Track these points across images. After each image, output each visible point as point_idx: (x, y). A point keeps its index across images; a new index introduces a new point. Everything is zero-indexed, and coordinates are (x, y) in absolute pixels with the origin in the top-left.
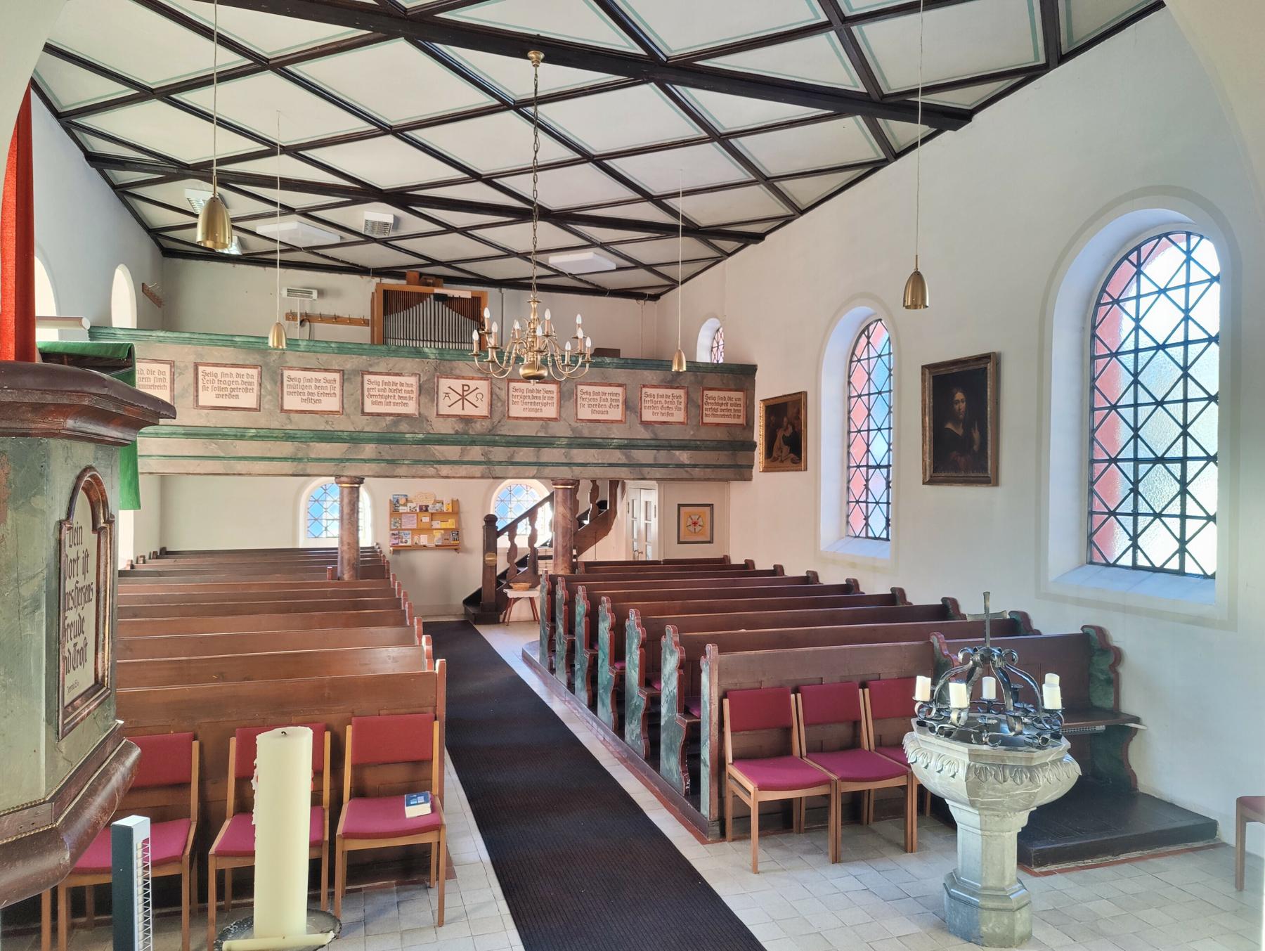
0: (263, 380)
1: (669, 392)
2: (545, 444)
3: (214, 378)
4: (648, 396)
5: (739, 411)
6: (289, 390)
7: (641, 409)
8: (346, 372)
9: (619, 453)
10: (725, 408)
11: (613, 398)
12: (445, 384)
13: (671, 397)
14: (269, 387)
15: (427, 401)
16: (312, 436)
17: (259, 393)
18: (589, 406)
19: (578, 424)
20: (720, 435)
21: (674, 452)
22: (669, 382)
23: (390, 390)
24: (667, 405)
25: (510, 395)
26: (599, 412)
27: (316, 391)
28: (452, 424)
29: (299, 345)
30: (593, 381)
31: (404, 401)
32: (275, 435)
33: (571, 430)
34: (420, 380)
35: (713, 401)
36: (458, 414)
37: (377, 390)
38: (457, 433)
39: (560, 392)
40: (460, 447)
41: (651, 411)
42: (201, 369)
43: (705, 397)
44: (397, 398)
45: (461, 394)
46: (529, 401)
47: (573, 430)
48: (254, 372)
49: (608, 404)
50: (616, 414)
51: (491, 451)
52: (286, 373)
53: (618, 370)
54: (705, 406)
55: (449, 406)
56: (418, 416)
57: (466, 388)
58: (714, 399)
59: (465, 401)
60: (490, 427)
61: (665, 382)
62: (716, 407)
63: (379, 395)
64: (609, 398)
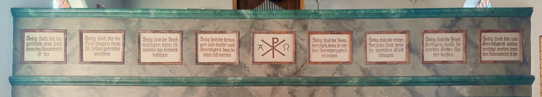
0: (126, 41)
1: (449, 35)
2: (340, 82)
3: (93, 41)
4: (429, 40)
5: (516, 49)
6: (145, 48)
7: (423, 51)
8: (184, 32)
9: (404, 90)
10: (502, 47)
11: (398, 43)
12: (258, 38)
13: (450, 40)
14: (130, 46)
15: (245, 51)
16: (159, 81)
17: (123, 51)
18: (377, 51)
19: (368, 66)
20: (500, 71)
21: (454, 86)
22: (449, 27)
23: (217, 45)
24: (447, 47)
26: (386, 56)
27: (163, 48)
29: (150, 13)
30: (380, 30)
32: (133, 81)
33: (362, 71)
34: (239, 36)
35: (490, 42)
38: (268, 75)
39: (352, 40)
40: (272, 87)
41: (432, 52)
42: (84, 35)
43: (482, 39)
44: (222, 50)
45: (271, 45)
46: (327, 49)
47: (363, 71)
48: (120, 35)
49: (393, 48)
50: (401, 56)
51: (296, 90)
52: (142, 35)
53: (403, 20)
54: (482, 47)
55: (263, 55)
56: (238, 64)
57: (275, 40)
58: (491, 39)
59: (275, 50)
60: (295, 70)
61: (445, 27)
62: (493, 47)
63: (209, 49)
64: (394, 43)
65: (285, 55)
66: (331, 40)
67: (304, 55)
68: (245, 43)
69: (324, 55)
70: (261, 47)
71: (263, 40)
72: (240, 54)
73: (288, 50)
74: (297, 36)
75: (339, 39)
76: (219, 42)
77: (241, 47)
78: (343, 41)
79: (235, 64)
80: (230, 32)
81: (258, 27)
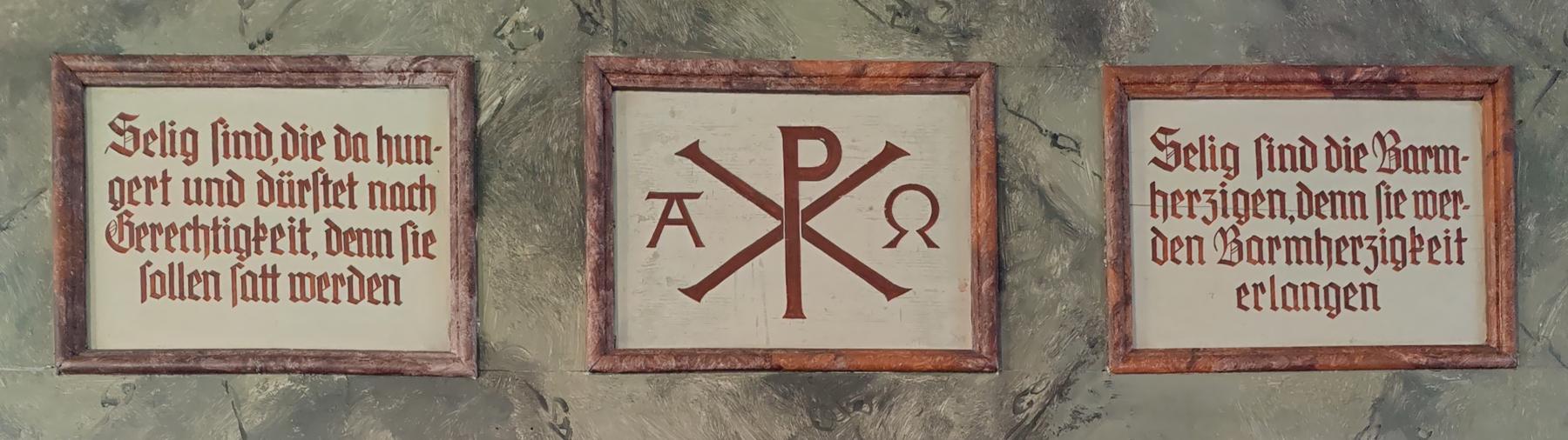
15: (526, 251)
23: (271, 190)
25: (1139, 196)
28: (715, 417)
31: (370, 266)
34: (473, 101)
36: (759, 343)
37: (176, 189)
44: (316, 240)
45: (778, 196)
46: (1281, 228)
55: (697, 292)
57: (812, 153)
63: (195, 225)
65: (902, 291)
66: (1322, 146)
67: (1074, 291)
68: (532, 172)
69: (1259, 287)
70: (675, 213)
71: (703, 149)
72: (487, 274)
73: (930, 244)
74: (1013, 106)
75: (1390, 141)
76: (283, 165)
77: (489, 209)
78: (1431, 163)
79: (436, 368)
80: (383, 62)
81: (650, 27)
